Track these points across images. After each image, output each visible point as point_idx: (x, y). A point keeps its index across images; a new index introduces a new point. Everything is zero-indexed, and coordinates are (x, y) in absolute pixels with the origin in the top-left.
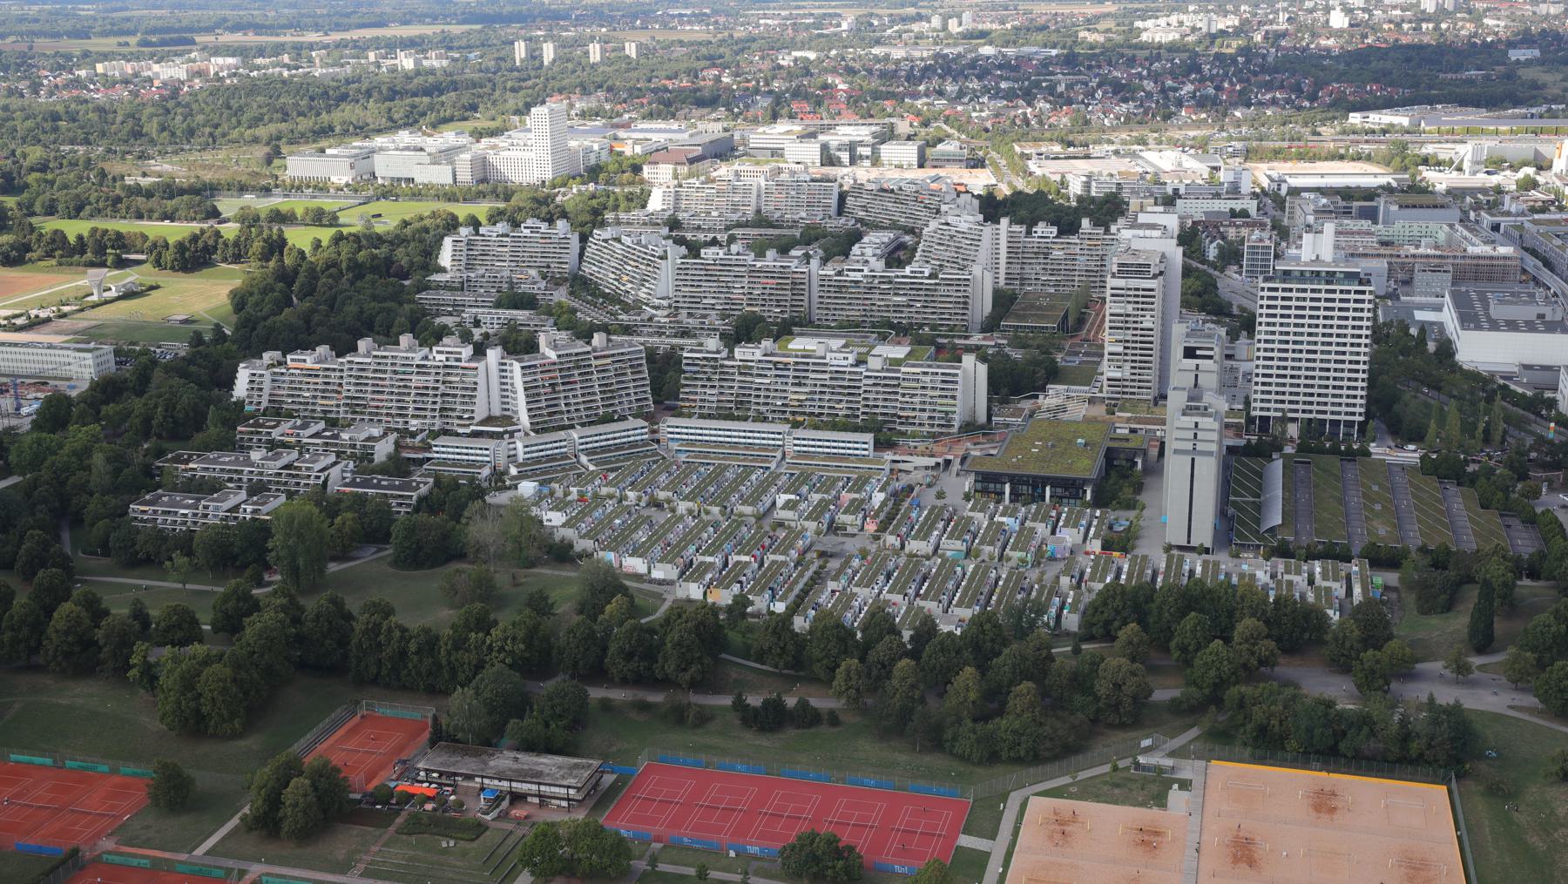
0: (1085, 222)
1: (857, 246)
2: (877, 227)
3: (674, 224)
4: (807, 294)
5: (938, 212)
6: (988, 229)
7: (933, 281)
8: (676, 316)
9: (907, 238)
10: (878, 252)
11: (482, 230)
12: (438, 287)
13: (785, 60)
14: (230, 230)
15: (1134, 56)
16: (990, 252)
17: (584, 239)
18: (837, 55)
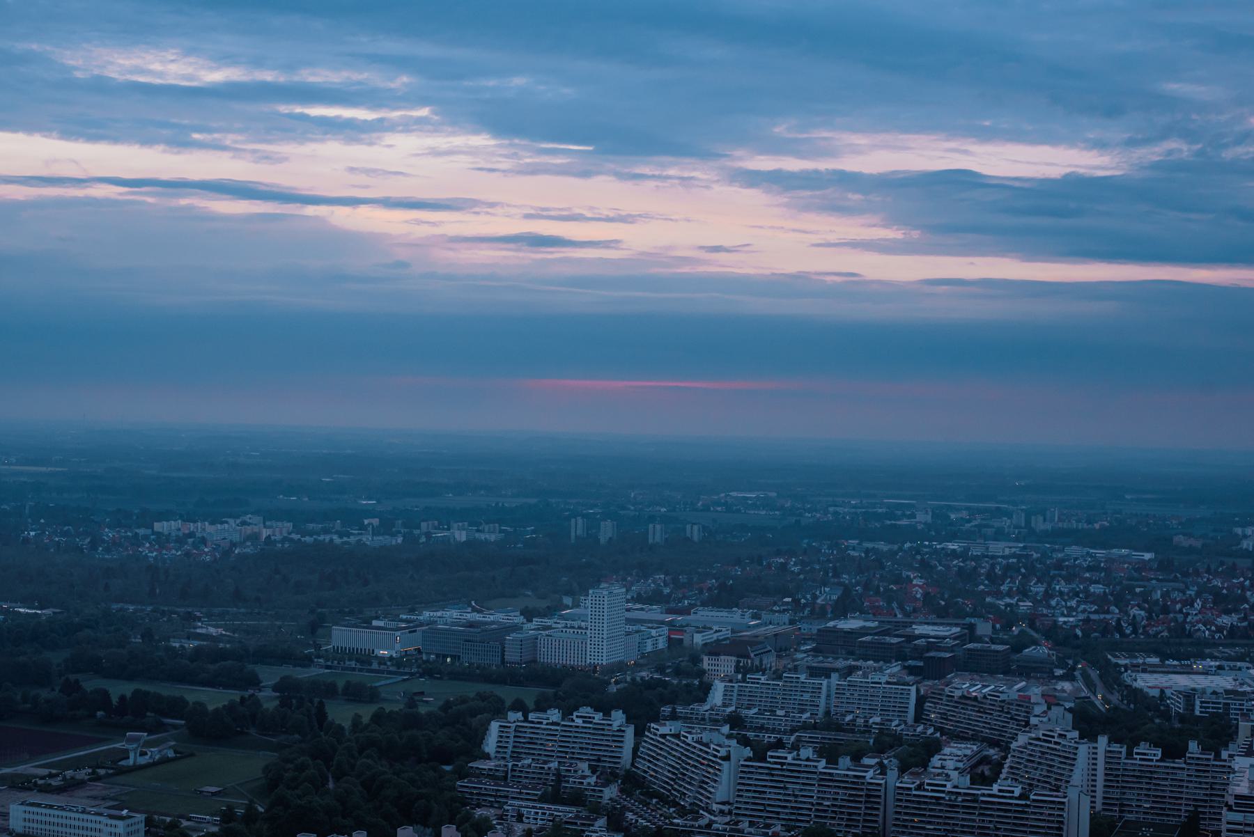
0: (1193, 746)
1: (937, 757)
2: (960, 737)
3: (735, 721)
4: (882, 808)
5: (1027, 724)
6: (1083, 750)
7: (1023, 802)
8: (737, 823)
9: (992, 752)
10: (960, 765)
11: (531, 716)
12: (480, 774)
13: (855, 548)
14: (268, 699)
15: (1234, 564)
16: (1086, 772)
17: (639, 733)
18: (910, 548)
